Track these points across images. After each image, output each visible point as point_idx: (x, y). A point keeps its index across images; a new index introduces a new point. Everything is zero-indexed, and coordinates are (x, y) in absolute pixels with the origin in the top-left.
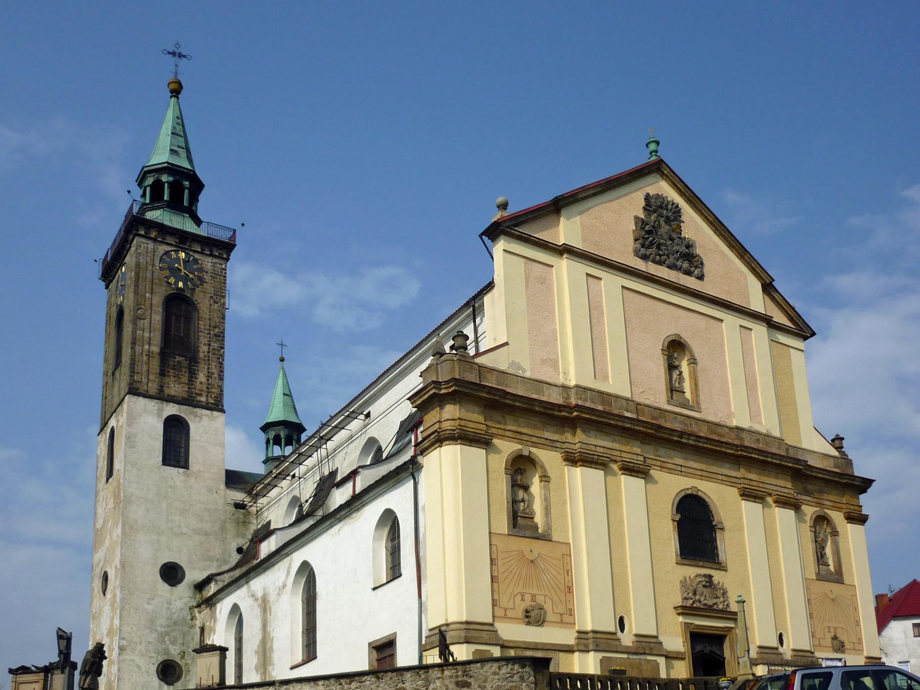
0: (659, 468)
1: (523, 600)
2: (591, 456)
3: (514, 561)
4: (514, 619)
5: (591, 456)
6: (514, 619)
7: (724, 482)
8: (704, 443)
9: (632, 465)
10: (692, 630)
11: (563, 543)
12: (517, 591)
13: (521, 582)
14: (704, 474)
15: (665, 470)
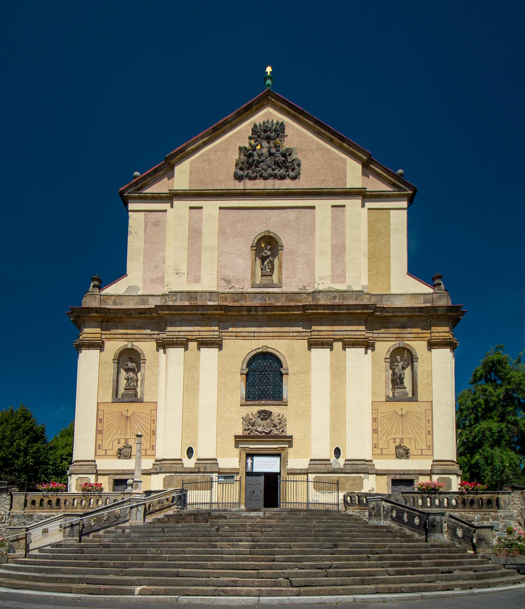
0: (234, 338)
1: (119, 443)
2: (171, 340)
3: (115, 419)
4: (111, 456)
5: (171, 340)
6: (111, 456)
8: (272, 311)
9: (205, 339)
10: (248, 452)
11: (152, 402)
12: (115, 438)
13: (119, 432)
14: (276, 334)
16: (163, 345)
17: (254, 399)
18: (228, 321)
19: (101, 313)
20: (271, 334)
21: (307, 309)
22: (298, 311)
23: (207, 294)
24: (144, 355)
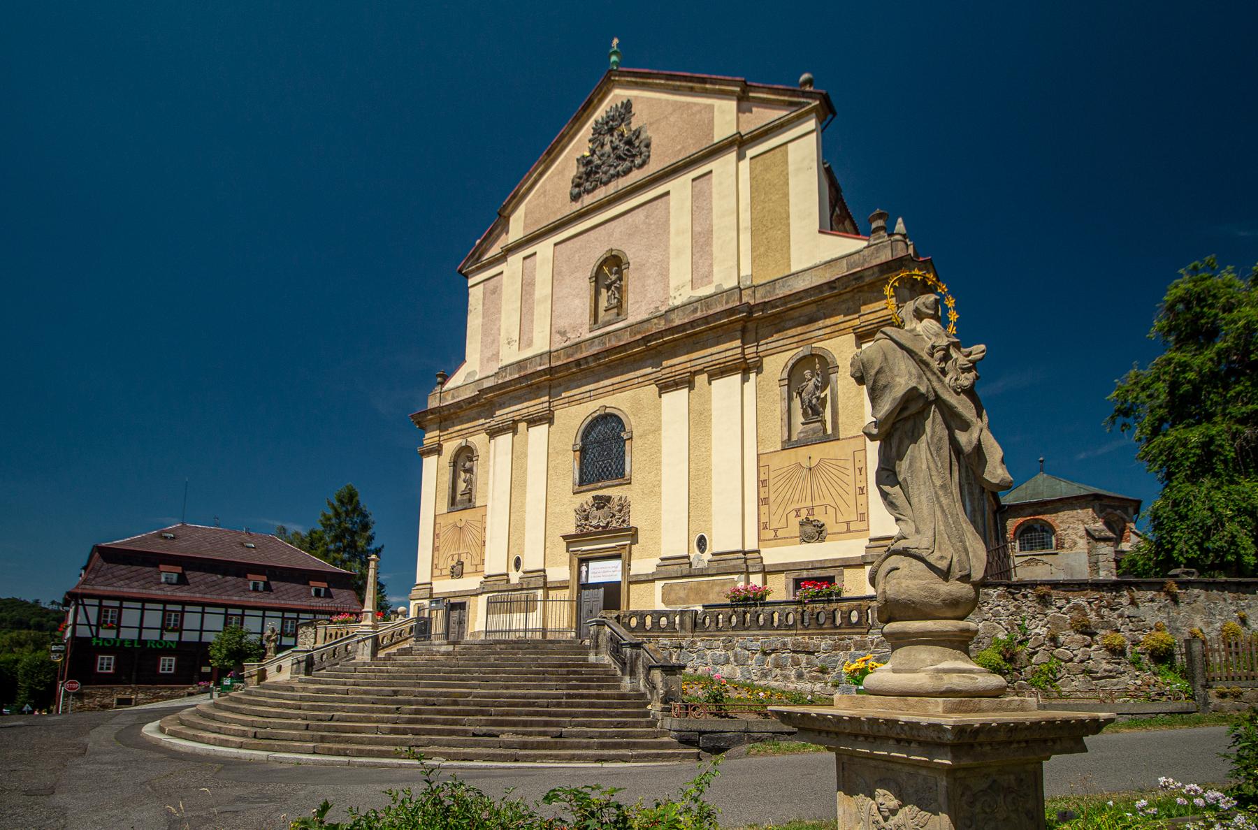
0: (567, 405)
7: (640, 385)
8: (605, 358)
15: (574, 403)
16: (493, 433)
17: (590, 482)
18: (560, 385)
19: (436, 413)
20: (611, 388)
21: (649, 341)
22: (639, 347)
23: (538, 358)
24: (477, 452)
